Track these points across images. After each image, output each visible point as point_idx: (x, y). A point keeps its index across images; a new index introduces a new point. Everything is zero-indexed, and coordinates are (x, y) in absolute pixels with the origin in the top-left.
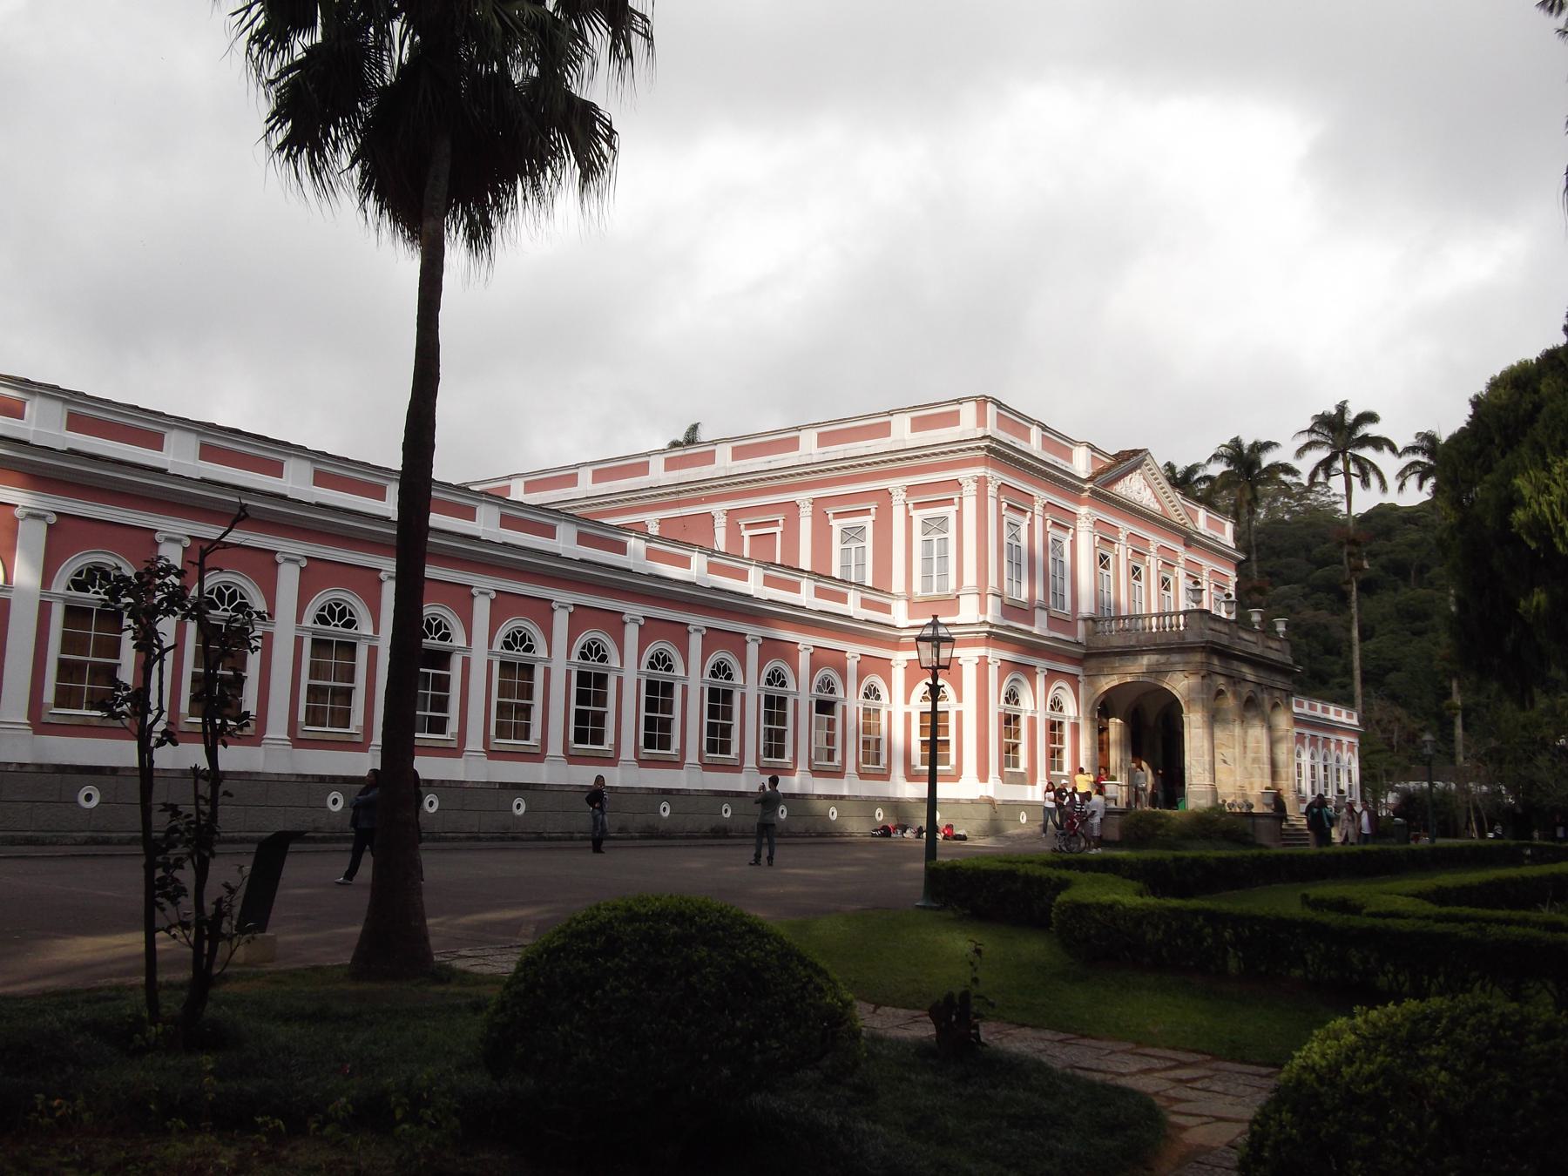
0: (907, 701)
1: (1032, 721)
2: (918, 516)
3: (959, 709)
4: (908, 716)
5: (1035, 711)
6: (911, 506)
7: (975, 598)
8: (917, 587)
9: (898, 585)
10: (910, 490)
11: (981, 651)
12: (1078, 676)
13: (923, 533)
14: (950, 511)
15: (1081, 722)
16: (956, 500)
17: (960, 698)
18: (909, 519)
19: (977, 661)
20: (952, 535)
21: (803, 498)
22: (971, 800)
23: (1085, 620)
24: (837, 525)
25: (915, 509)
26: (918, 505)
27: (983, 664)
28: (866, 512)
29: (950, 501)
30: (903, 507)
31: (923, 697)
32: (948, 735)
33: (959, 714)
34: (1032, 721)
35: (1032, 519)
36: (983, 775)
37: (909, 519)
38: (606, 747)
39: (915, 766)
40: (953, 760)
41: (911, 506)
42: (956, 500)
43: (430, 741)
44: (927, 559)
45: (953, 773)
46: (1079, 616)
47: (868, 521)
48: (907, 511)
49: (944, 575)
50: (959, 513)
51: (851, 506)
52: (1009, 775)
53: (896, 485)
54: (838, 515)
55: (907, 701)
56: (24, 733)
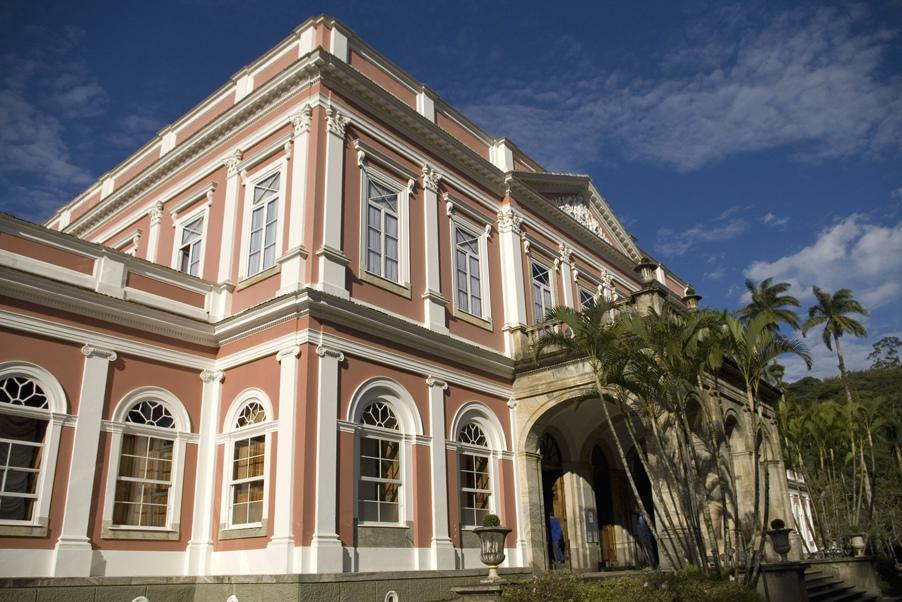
0: (221, 430)
1: (422, 453)
3: (274, 430)
4: (221, 449)
5: (425, 436)
8: (243, 273)
9: (224, 275)
10: (242, 156)
11: (303, 336)
12: (507, 400)
17: (276, 415)
19: (297, 351)
20: (281, 194)
22: (277, 577)
23: (512, 331)
27: (308, 357)
33: (275, 435)
34: (422, 453)
35: (417, 188)
36: (303, 535)
44: (255, 233)
49: (270, 246)
52: (369, 532)
55: (221, 430)
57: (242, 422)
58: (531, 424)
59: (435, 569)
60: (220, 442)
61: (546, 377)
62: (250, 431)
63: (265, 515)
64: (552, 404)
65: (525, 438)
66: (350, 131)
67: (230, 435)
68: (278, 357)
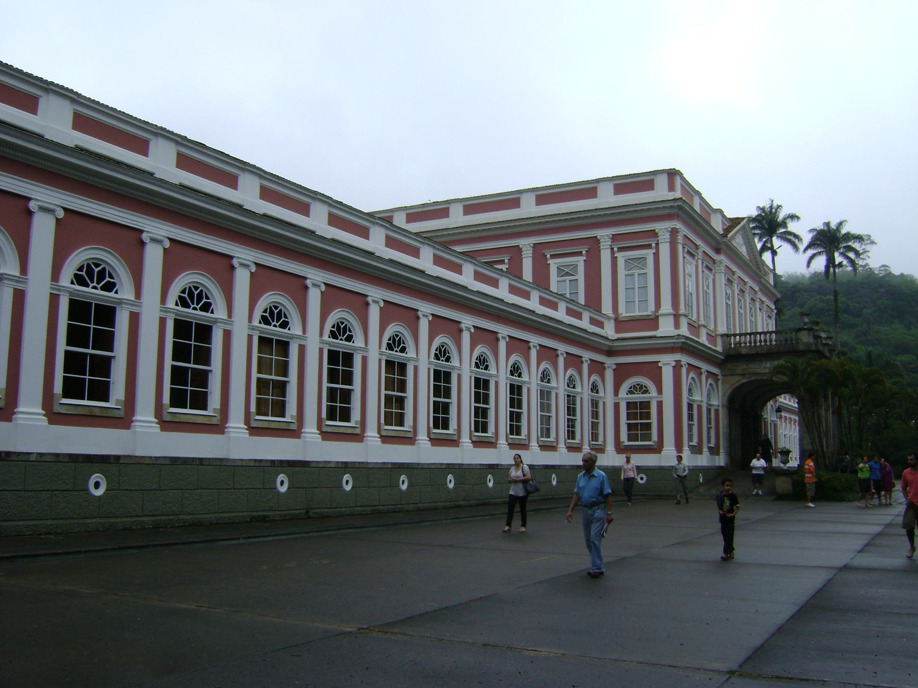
0: (616, 393)
2: (621, 257)
4: (617, 406)
6: (615, 249)
7: (671, 319)
10: (615, 238)
11: (678, 356)
13: (625, 270)
14: (649, 254)
15: (720, 408)
16: (654, 245)
17: (660, 391)
18: (614, 260)
19: (674, 364)
21: (526, 244)
23: (722, 336)
24: (553, 264)
25: (618, 251)
26: (621, 249)
27: (677, 367)
28: (579, 254)
29: (649, 246)
30: (609, 250)
31: (628, 391)
32: (650, 419)
33: (660, 404)
37: (614, 260)
38: (450, 431)
39: (624, 442)
40: (655, 437)
41: (615, 249)
42: (654, 245)
43: (400, 432)
45: (655, 447)
46: (718, 333)
47: (580, 261)
48: (613, 252)
50: (656, 256)
51: (565, 249)
53: (604, 234)
54: (553, 256)
55: (616, 393)
56: (152, 430)
57: (630, 392)
58: (731, 390)
59: (706, 465)
60: (617, 401)
61: (741, 367)
62: (638, 397)
63: (655, 437)
64: (745, 381)
65: (726, 398)
66: (725, 276)
67: (626, 399)
68: (660, 365)
